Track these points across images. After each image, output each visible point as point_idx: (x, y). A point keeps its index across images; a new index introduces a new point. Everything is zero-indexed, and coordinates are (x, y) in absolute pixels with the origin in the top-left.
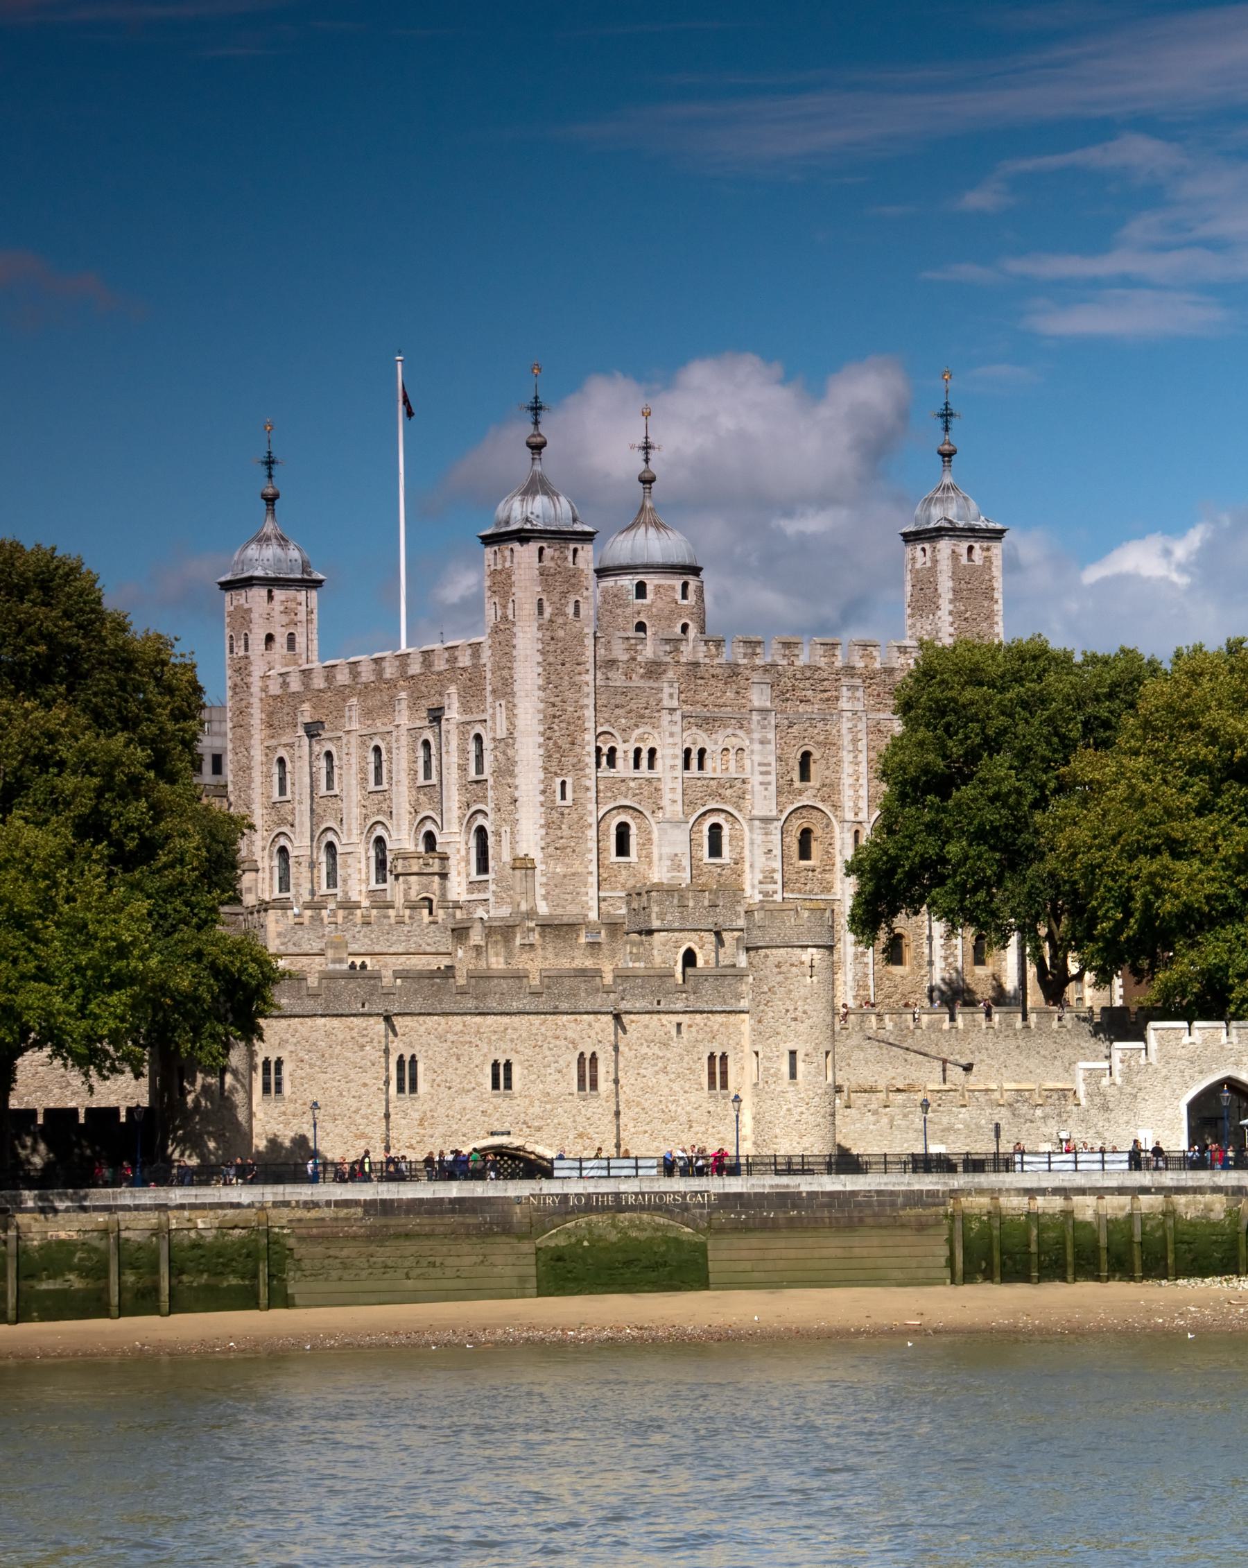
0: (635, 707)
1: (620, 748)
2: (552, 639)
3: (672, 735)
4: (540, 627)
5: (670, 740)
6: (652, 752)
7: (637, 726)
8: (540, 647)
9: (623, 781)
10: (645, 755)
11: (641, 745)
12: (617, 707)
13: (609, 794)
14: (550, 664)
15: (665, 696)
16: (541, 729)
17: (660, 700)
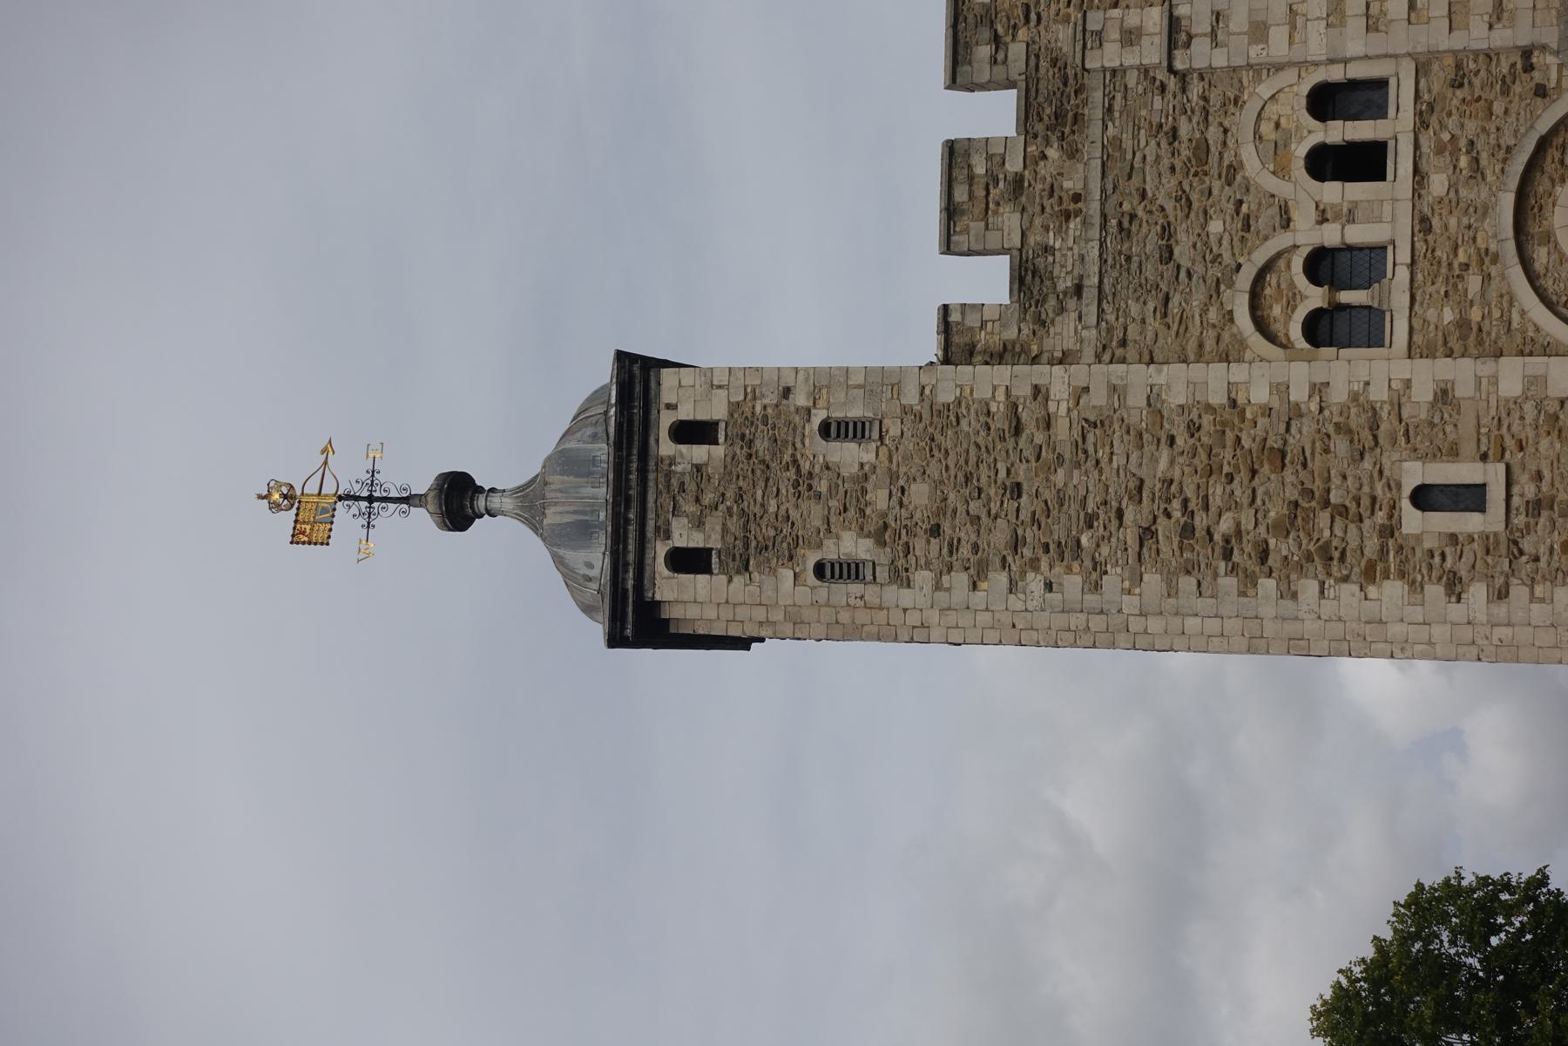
0: (1170, 183)
1: (1307, 234)
2: (935, 531)
3: (1259, 32)
4: (901, 577)
5: (1278, 36)
6: (1324, 102)
7: (1232, 172)
8: (960, 579)
9: (1423, 224)
10: (1338, 132)
11: (1301, 150)
12: (1167, 255)
13: (1474, 283)
14: (1016, 544)
15: (1131, 59)
17: (1145, 71)
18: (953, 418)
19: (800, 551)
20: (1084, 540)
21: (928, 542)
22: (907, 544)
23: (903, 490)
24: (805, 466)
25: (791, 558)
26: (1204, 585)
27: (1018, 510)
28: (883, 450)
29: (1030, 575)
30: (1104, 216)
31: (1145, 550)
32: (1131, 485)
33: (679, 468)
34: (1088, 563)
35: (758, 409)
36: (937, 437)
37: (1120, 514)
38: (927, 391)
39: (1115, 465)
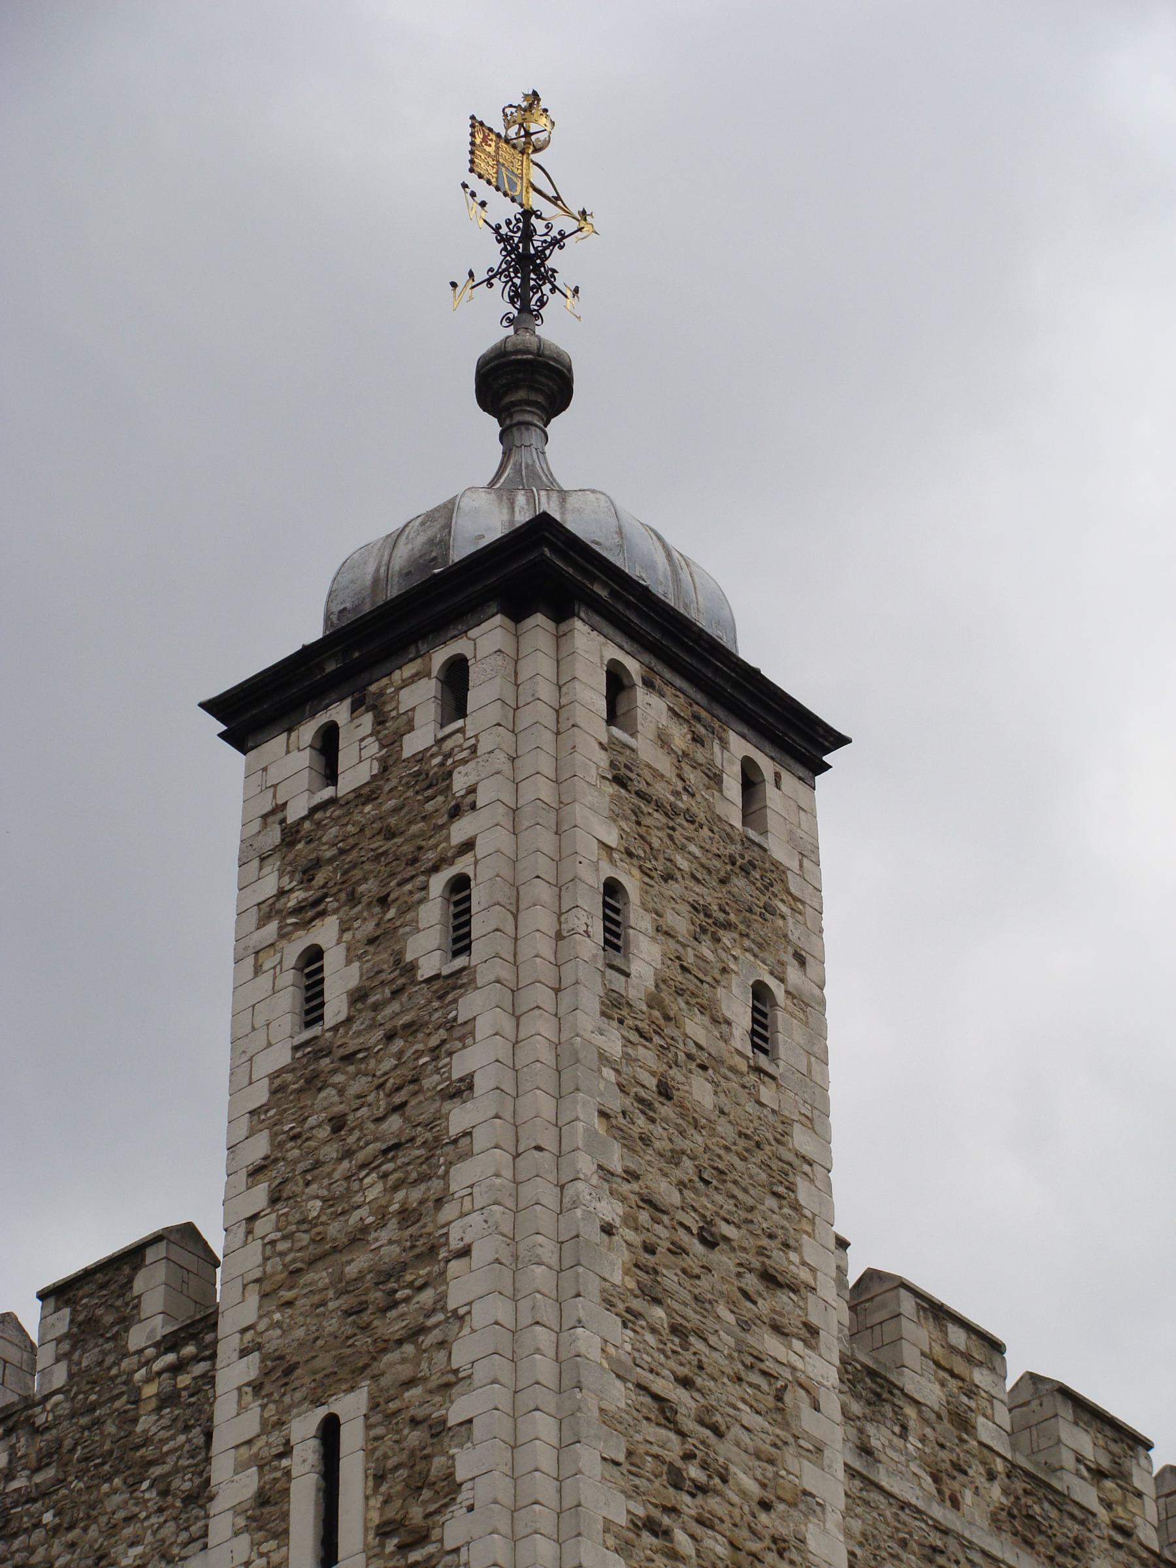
16: (619, 1510)
18: (781, 1190)
19: (636, 872)
20: (659, 1313)
21: (653, 1074)
22: (650, 1040)
23: (704, 1068)
24: (727, 938)
25: (630, 854)
26: (614, 1470)
27: (688, 1229)
28: (743, 1066)
29: (620, 1208)
30: (945, 1532)
31: (648, 1400)
32: (718, 1418)
33: (717, 748)
34: (638, 1304)
35: (784, 909)
36: (759, 1156)
37: (686, 1383)
38: (806, 1168)
39: (741, 1405)
